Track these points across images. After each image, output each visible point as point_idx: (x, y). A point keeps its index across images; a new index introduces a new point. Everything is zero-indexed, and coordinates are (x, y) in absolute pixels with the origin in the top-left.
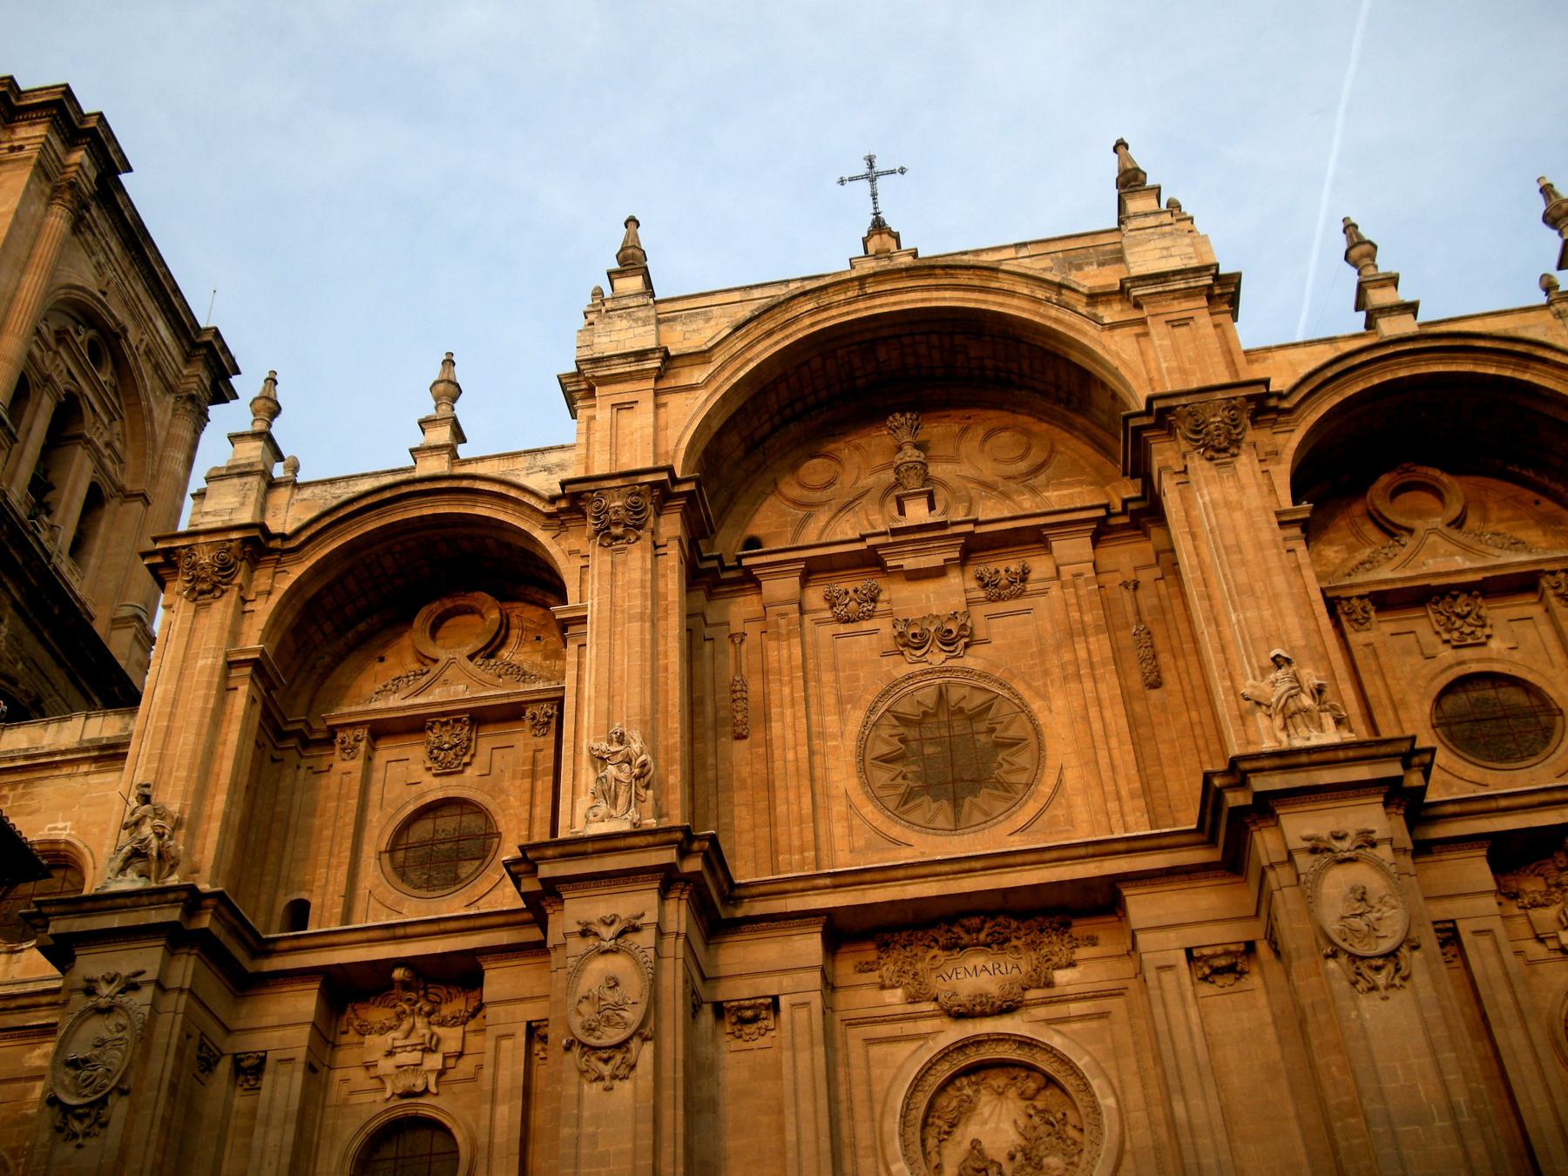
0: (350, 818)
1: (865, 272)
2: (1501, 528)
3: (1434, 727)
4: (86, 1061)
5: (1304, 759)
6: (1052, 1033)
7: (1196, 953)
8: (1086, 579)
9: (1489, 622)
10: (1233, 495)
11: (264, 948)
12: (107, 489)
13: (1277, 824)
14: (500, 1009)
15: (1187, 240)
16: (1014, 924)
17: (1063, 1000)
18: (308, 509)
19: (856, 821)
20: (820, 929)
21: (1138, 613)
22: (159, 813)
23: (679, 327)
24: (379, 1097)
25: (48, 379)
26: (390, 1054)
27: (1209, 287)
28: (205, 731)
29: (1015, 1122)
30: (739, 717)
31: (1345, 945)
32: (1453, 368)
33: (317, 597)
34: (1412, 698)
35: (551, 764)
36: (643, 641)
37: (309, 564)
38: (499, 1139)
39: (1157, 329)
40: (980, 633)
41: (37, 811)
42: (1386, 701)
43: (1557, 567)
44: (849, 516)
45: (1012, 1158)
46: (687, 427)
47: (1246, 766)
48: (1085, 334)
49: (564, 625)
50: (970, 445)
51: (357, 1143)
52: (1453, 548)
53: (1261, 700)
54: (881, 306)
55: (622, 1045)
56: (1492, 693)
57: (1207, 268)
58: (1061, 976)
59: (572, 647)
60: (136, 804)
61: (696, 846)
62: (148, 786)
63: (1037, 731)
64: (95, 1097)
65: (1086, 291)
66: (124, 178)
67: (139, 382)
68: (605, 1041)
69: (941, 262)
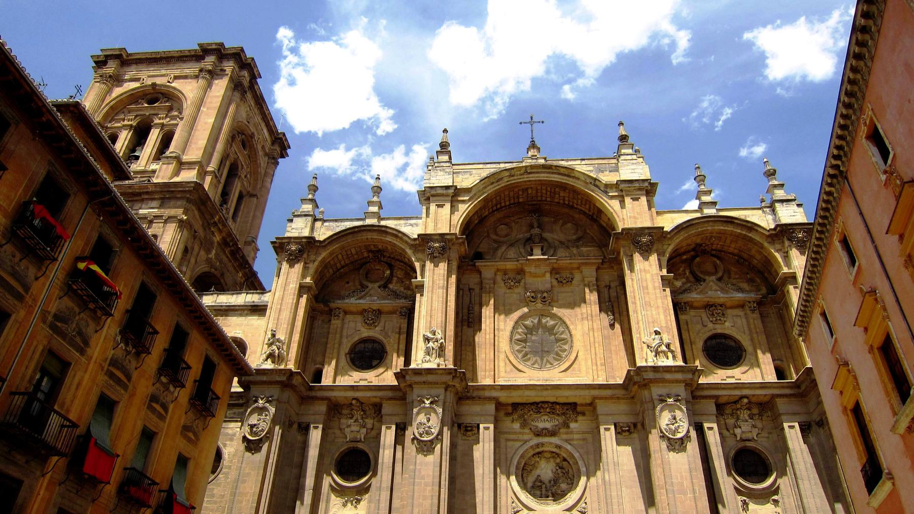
0: (337, 341)
1: (527, 164)
2: (734, 282)
3: (703, 351)
4: (255, 425)
5: (661, 369)
6: (567, 444)
7: (617, 425)
8: (593, 285)
9: (726, 315)
10: (647, 268)
11: (311, 389)
12: (244, 193)
13: (650, 389)
14: (387, 417)
15: (641, 167)
16: (558, 407)
17: (572, 433)
18: (328, 230)
19: (508, 361)
20: (495, 402)
21: (610, 297)
22: (279, 341)
23: (460, 176)
24: (345, 440)
25: (228, 155)
26: (349, 426)
27: (647, 187)
28: (293, 311)
29: (552, 470)
30: (471, 320)
31: (667, 434)
32: (726, 228)
33: (329, 262)
34: (697, 340)
35: (405, 330)
36: (443, 296)
37: (328, 252)
38: (385, 461)
39: (628, 200)
40: (555, 298)
41: (229, 326)
42: (689, 341)
43: (751, 300)
44: (513, 248)
45: (550, 482)
46: (461, 216)
47: (642, 370)
48: (602, 199)
49: (417, 287)
50: (557, 227)
51: (337, 455)
52: (718, 288)
53: (649, 345)
54: (532, 177)
55: (431, 441)
56: (724, 340)
57: (647, 180)
58: (573, 425)
59: (418, 296)
60: (270, 336)
61: (458, 375)
62: (275, 331)
63: (571, 335)
64: (257, 438)
65: (604, 182)
66: (259, 80)
67: (257, 154)
68: (425, 439)
69: (555, 163)
